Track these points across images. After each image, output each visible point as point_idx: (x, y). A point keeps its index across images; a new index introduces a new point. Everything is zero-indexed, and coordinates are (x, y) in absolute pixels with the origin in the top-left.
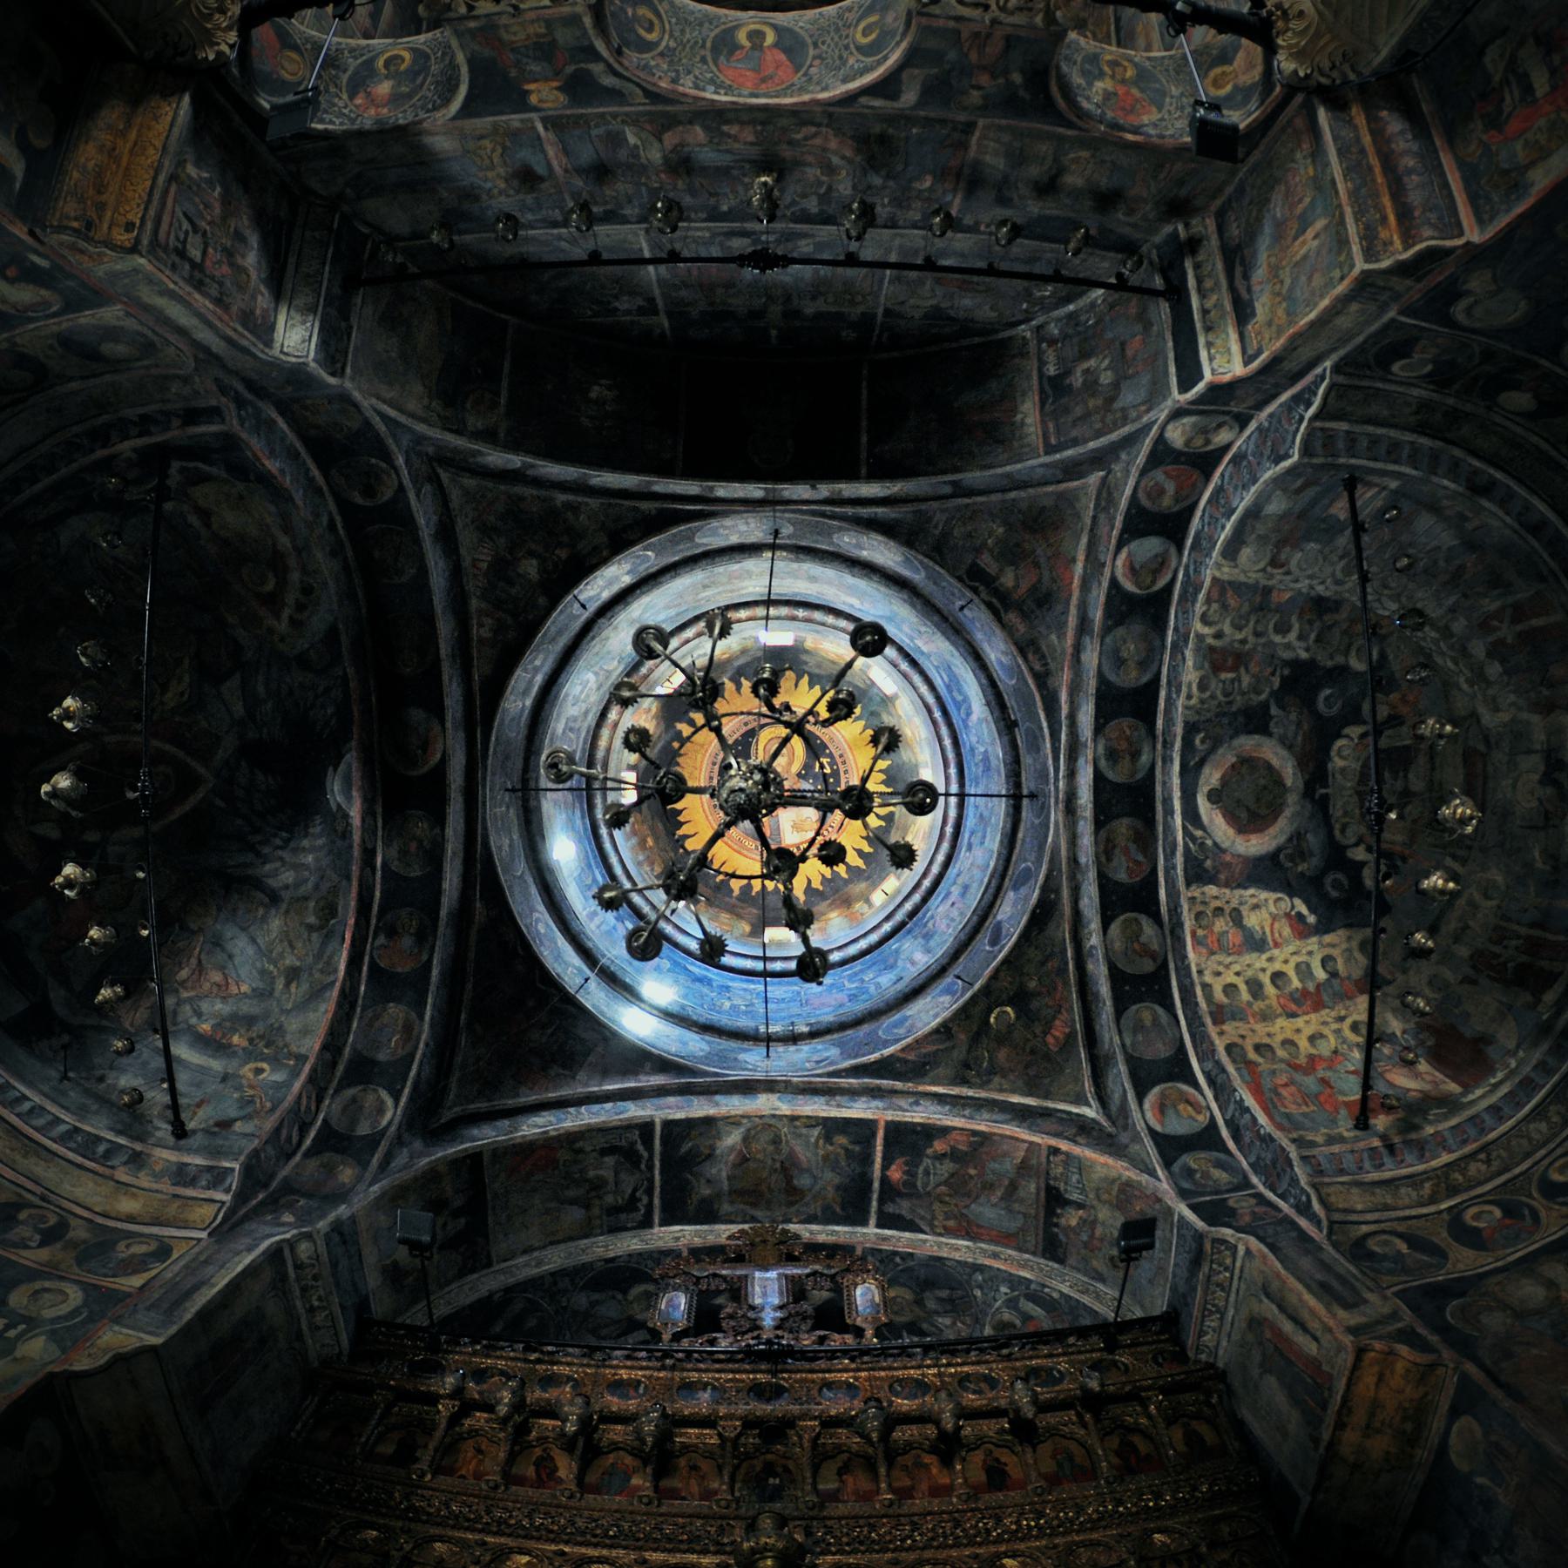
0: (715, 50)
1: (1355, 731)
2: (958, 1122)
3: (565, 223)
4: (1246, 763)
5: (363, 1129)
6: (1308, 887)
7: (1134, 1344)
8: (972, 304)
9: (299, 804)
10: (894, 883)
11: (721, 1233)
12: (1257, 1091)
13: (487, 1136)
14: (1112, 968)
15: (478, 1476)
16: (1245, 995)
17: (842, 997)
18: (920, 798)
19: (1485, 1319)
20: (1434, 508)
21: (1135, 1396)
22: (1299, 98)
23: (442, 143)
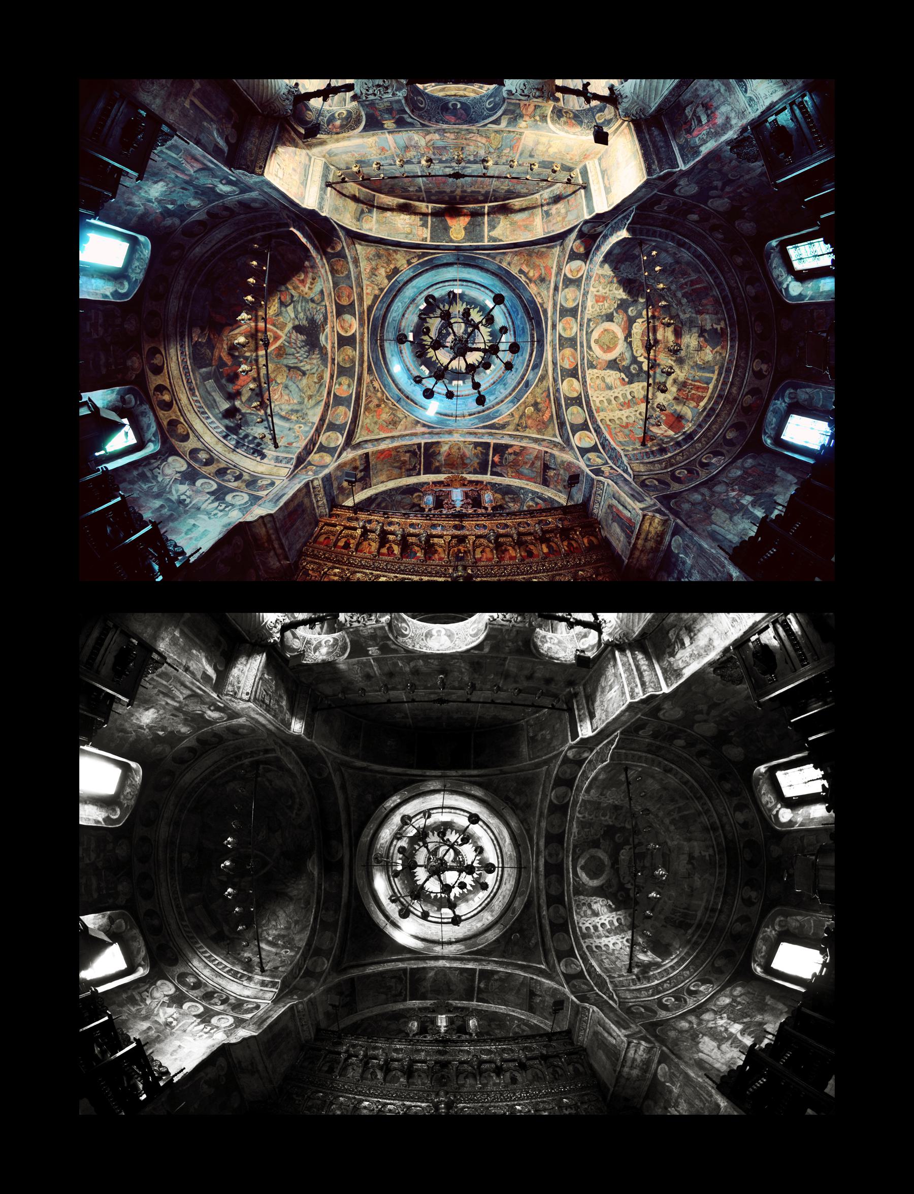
0: (426, 636)
1: (627, 847)
2: (502, 969)
3: (380, 691)
4: (593, 857)
5: (318, 970)
7: (557, 1039)
8: (507, 714)
9: (298, 870)
10: (482, 895)
11: (428, 1003)
12: (597, 960)
13: (355, 973)
14: (550, 922)
15: (353, 1077)
16: (592, 930)
17: (466, 930)
18: (490, 868)
19: (669, 1033)
20: (653, 777)
21: (557, 1056)
22: (610, 648)
23: (342, 667)
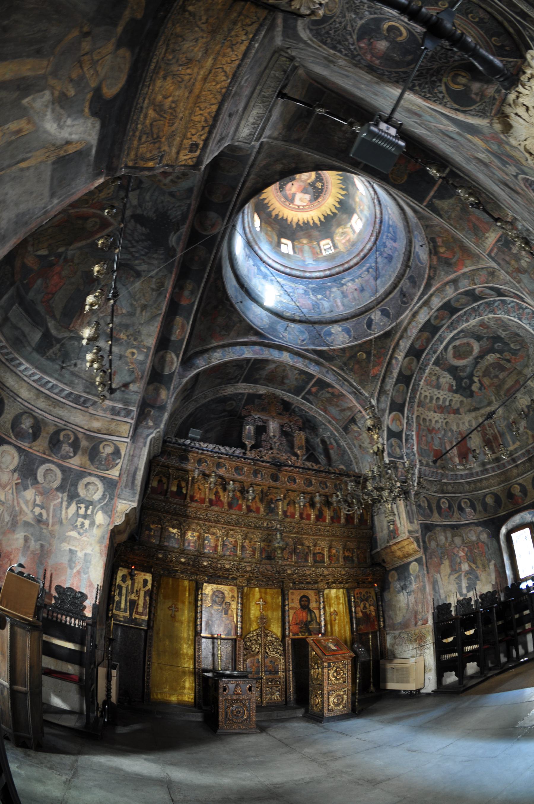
1: (498, 355)
6: (458, 379)
